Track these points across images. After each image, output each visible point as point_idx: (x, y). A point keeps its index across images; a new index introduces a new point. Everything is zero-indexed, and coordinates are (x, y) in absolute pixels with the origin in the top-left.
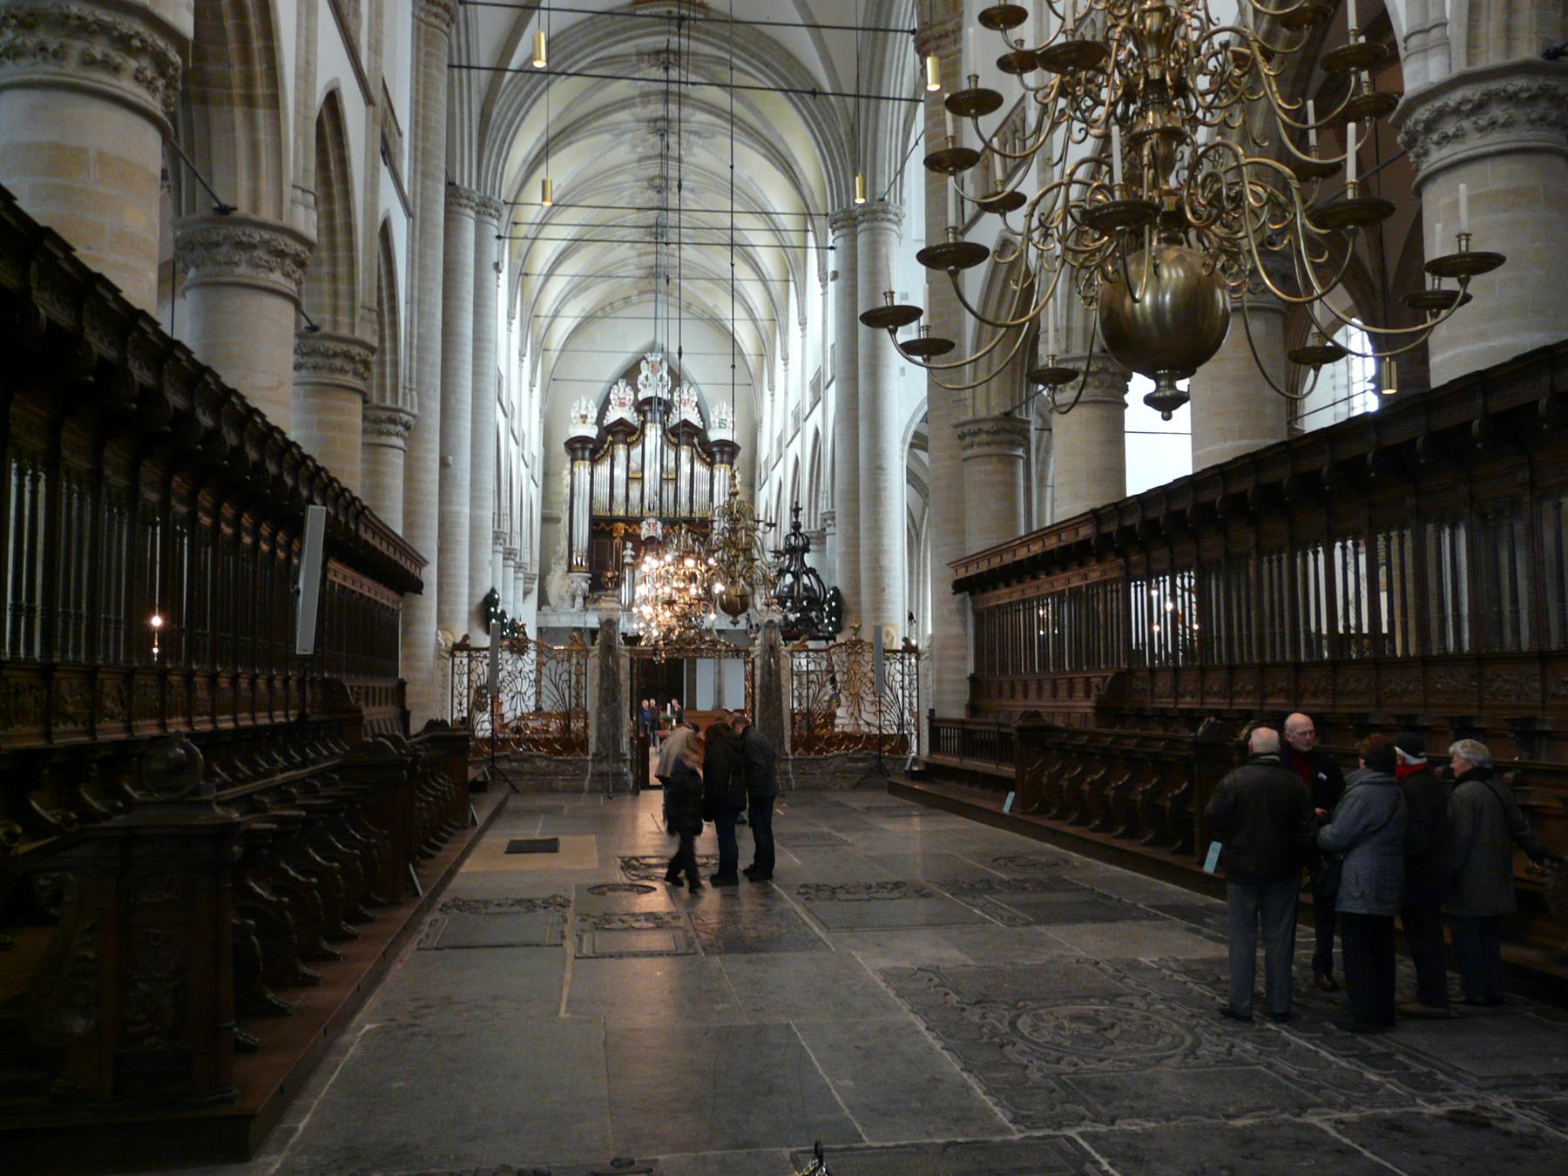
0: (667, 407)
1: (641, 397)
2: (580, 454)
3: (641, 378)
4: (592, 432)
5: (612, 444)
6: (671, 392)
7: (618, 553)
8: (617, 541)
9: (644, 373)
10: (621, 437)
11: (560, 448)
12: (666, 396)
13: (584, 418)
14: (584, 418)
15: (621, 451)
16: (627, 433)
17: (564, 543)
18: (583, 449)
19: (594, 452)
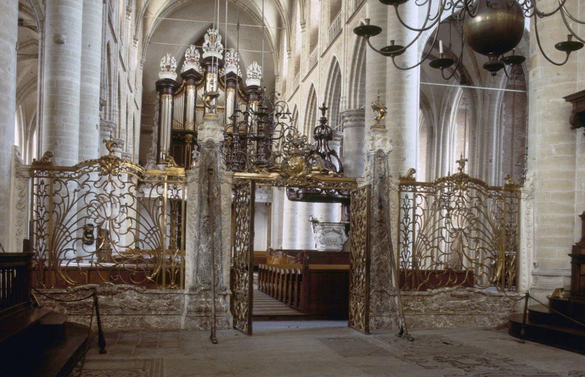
0: (222, 64)
1: (205, 56)
2: (165, 90)
3: (205, 45)
4: (173, 76)
5: (186, 85)
6: (223, 54)
7: (188, 153)
8: (188, 145)
9: (207, 41)
10: (191, 81)
11: (153, 87)
12: (221, 57)
13: (168, 67)
14: (168, 67)
15: (191, 91)
16: (198, 79)
17: (155, 145)
18: (168, 87)
19: (174, 89)
